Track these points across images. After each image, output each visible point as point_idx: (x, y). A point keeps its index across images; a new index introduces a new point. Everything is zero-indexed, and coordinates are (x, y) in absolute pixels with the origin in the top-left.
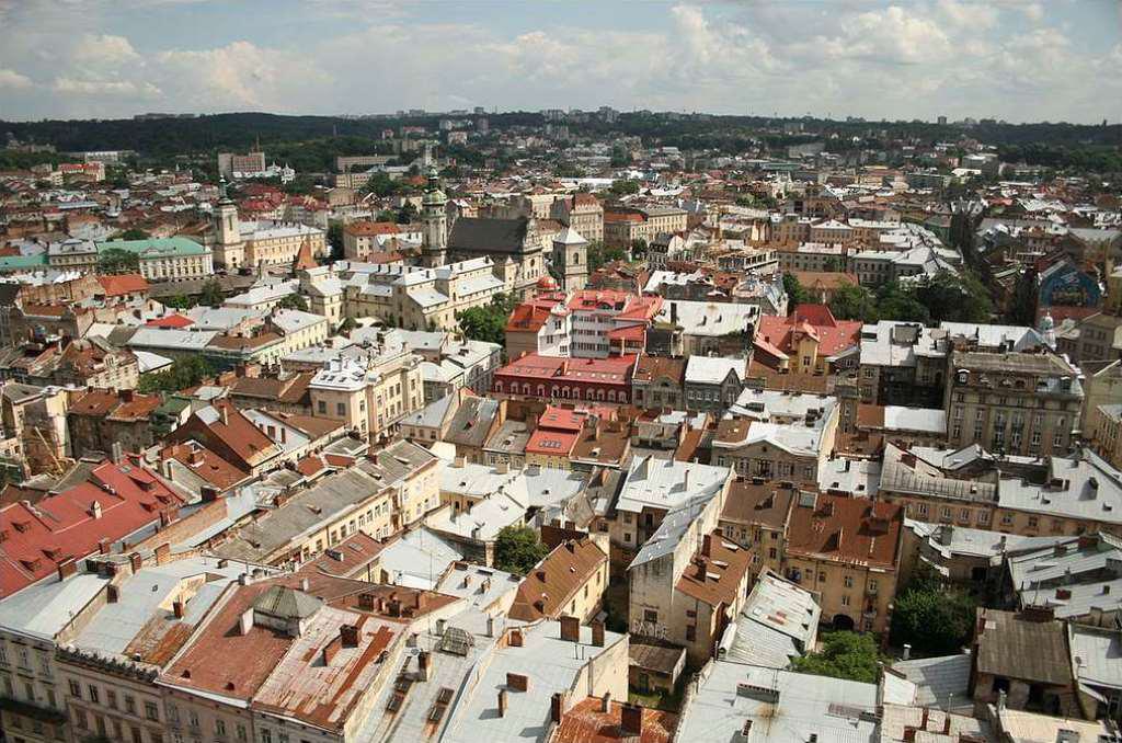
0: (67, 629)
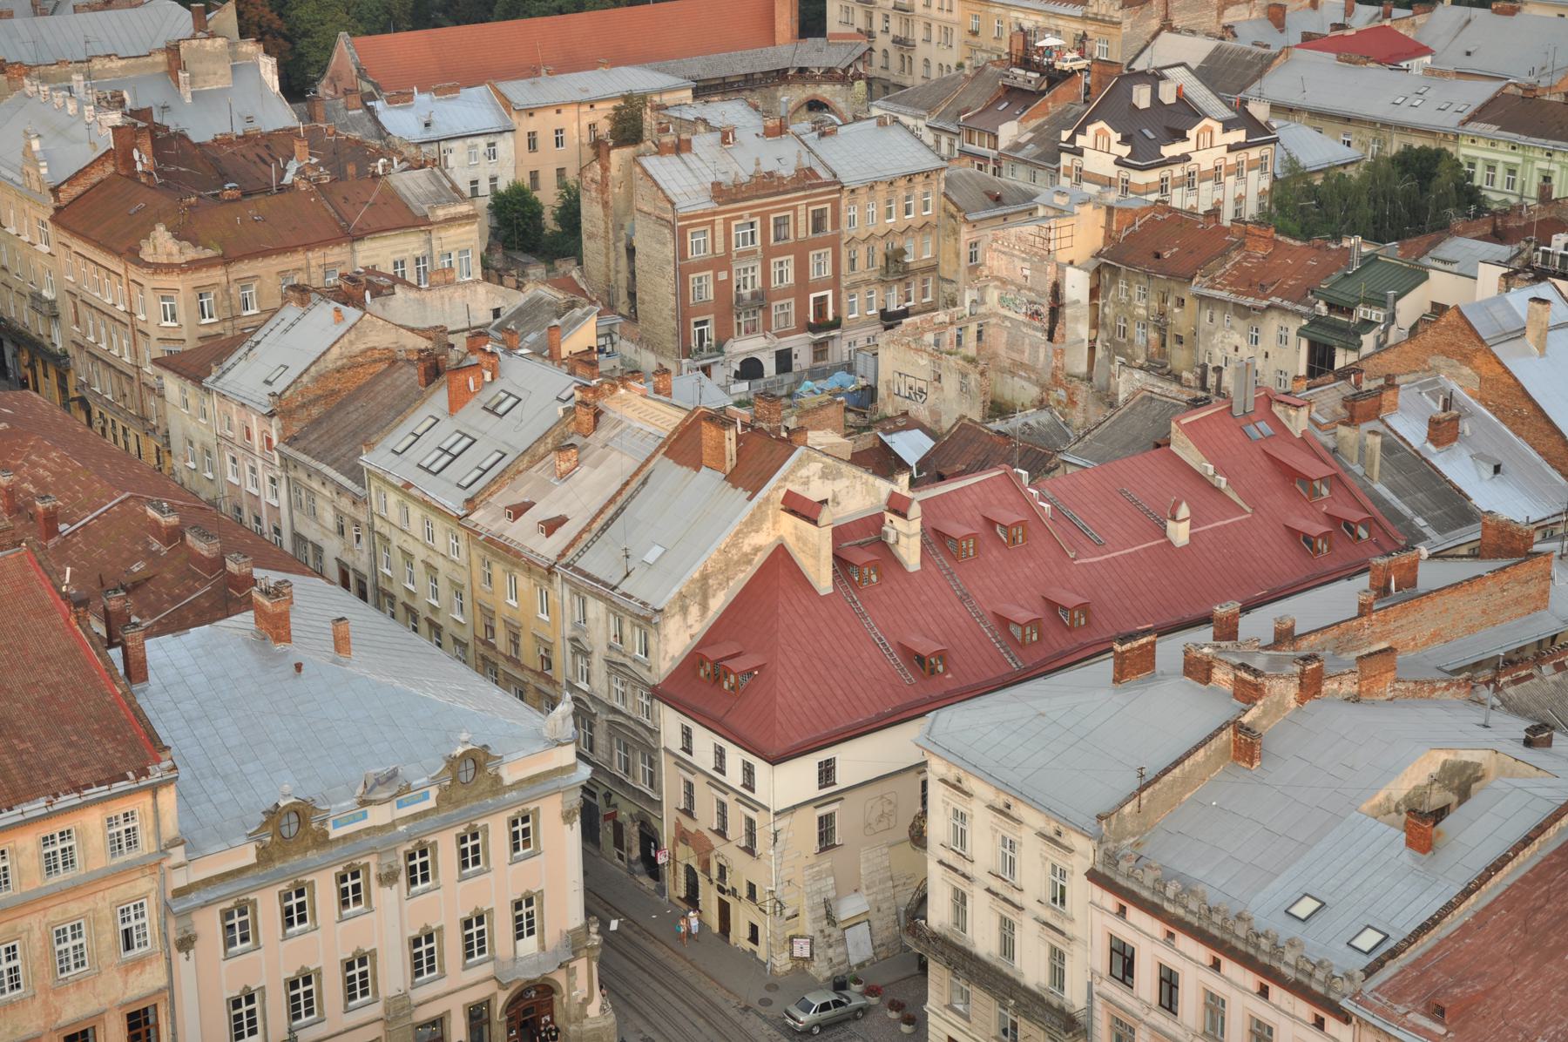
0: (1128, 809)
